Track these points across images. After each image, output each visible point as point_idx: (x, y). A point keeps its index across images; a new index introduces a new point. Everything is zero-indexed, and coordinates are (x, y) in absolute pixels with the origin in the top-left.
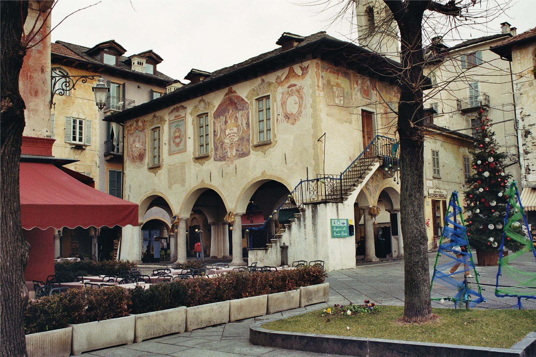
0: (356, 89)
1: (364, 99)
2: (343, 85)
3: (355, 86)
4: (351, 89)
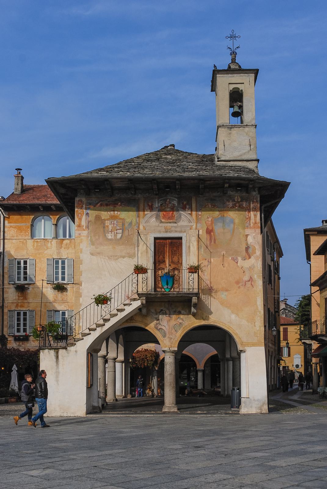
1: (161, 225)
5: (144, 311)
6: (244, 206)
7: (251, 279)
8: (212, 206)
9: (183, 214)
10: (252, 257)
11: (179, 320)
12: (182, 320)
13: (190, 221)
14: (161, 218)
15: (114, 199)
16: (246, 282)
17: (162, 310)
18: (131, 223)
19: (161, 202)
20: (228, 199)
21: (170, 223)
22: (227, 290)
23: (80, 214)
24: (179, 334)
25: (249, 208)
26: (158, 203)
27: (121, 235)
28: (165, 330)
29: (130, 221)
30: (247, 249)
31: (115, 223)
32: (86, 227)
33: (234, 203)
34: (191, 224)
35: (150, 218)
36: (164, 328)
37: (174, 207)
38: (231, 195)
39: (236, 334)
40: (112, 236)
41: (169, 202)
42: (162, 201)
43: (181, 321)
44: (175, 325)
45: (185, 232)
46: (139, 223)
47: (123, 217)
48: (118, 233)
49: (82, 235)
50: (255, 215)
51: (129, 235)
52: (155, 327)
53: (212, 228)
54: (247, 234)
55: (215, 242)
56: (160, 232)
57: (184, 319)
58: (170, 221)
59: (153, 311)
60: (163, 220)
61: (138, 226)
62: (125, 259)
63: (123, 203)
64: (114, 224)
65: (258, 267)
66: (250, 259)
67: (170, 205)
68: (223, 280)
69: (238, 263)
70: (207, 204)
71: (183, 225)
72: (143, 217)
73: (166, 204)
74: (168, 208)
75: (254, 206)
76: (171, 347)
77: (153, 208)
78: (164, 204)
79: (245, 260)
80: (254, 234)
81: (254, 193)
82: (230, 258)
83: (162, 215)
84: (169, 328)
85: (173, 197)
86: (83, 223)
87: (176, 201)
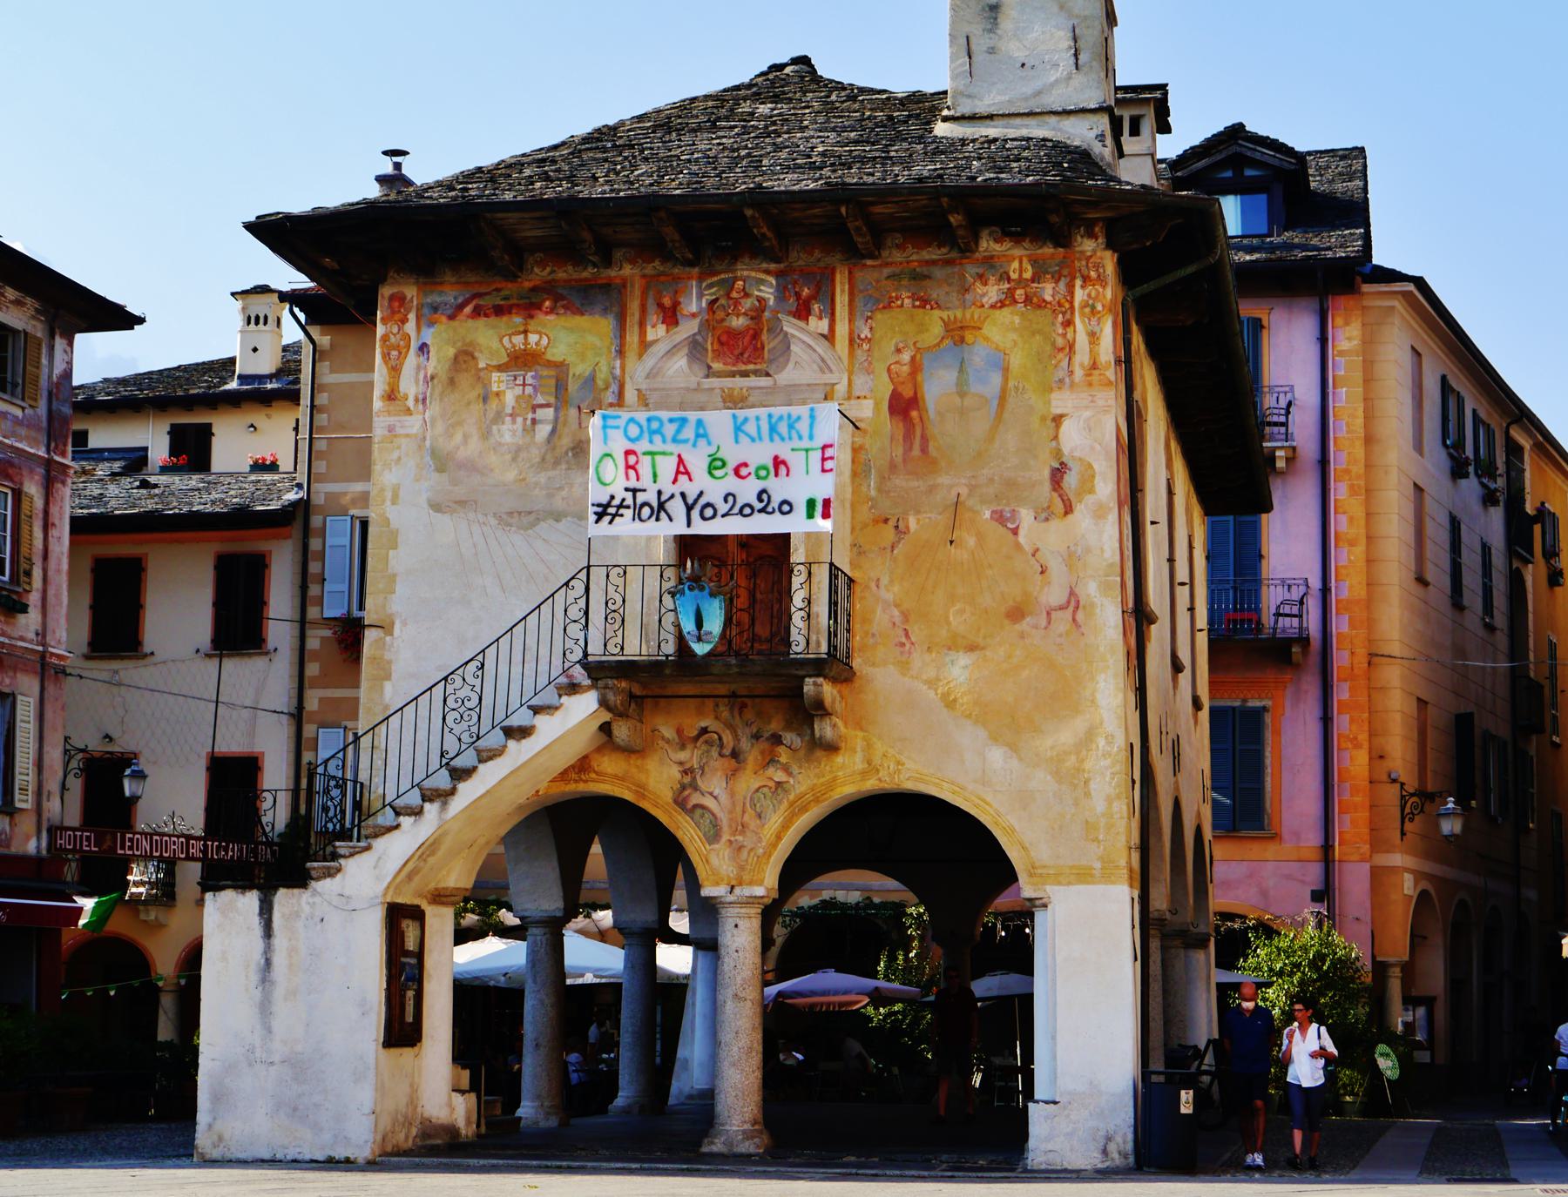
0: (659, 349)
2: (557, 353)
3: (657, 331)
4: (621, 353)
5: (622, 731)
6: (1048, 298)
7: (1073, 602)
10: (1079, 509)
11: (771, 771)
12: (786, 769)
13: (824, 367)
15: (527, 285)
16: (1054, 615)
17: (704, 731)
18: (591, 380)
20: (980, 271)
21: (745, 374)
22: (972, 648)
23: (397, 347)
24: (780, 832)
25: (1067, 305)
26: (700, 296)
27: (549, 428)
28: (719, 814)
30: (1058, 475)
31: (529, 380)
32: (417, 400)
34: (828, 378)
36: (708, 802)
38: (992, 257)
39: (1011, 831)
40: (514, 433)
43: (780, 776)
44: (757, 790)
47: (558, 358)
48: (541, 422)
49: (399, 431)
50: (1093, 337)
52: (676, 802)
54: (1059, 411)
55: (924, 450)
57: (795, 769)
58: (744, 367)
59: (668, 732)
62: (562, 525)
64: (524, 385)
65: (1102, 550)
66: (1070, 516)
67: (747, 304)
68: (958, 606)
69: (1022, 532)
72: (640, 356)
73: (729, 297)
74: (738, 316)
75: (1089, 295)
76: (740, 884)
78: (723, 301)
79: (1047, 519)
80: (1087, 414)
81: (1088, 245)
82: (987, 514)
84: (734, 804)
85: (759, 270)
86: (409, 386)
87: (771, 285)
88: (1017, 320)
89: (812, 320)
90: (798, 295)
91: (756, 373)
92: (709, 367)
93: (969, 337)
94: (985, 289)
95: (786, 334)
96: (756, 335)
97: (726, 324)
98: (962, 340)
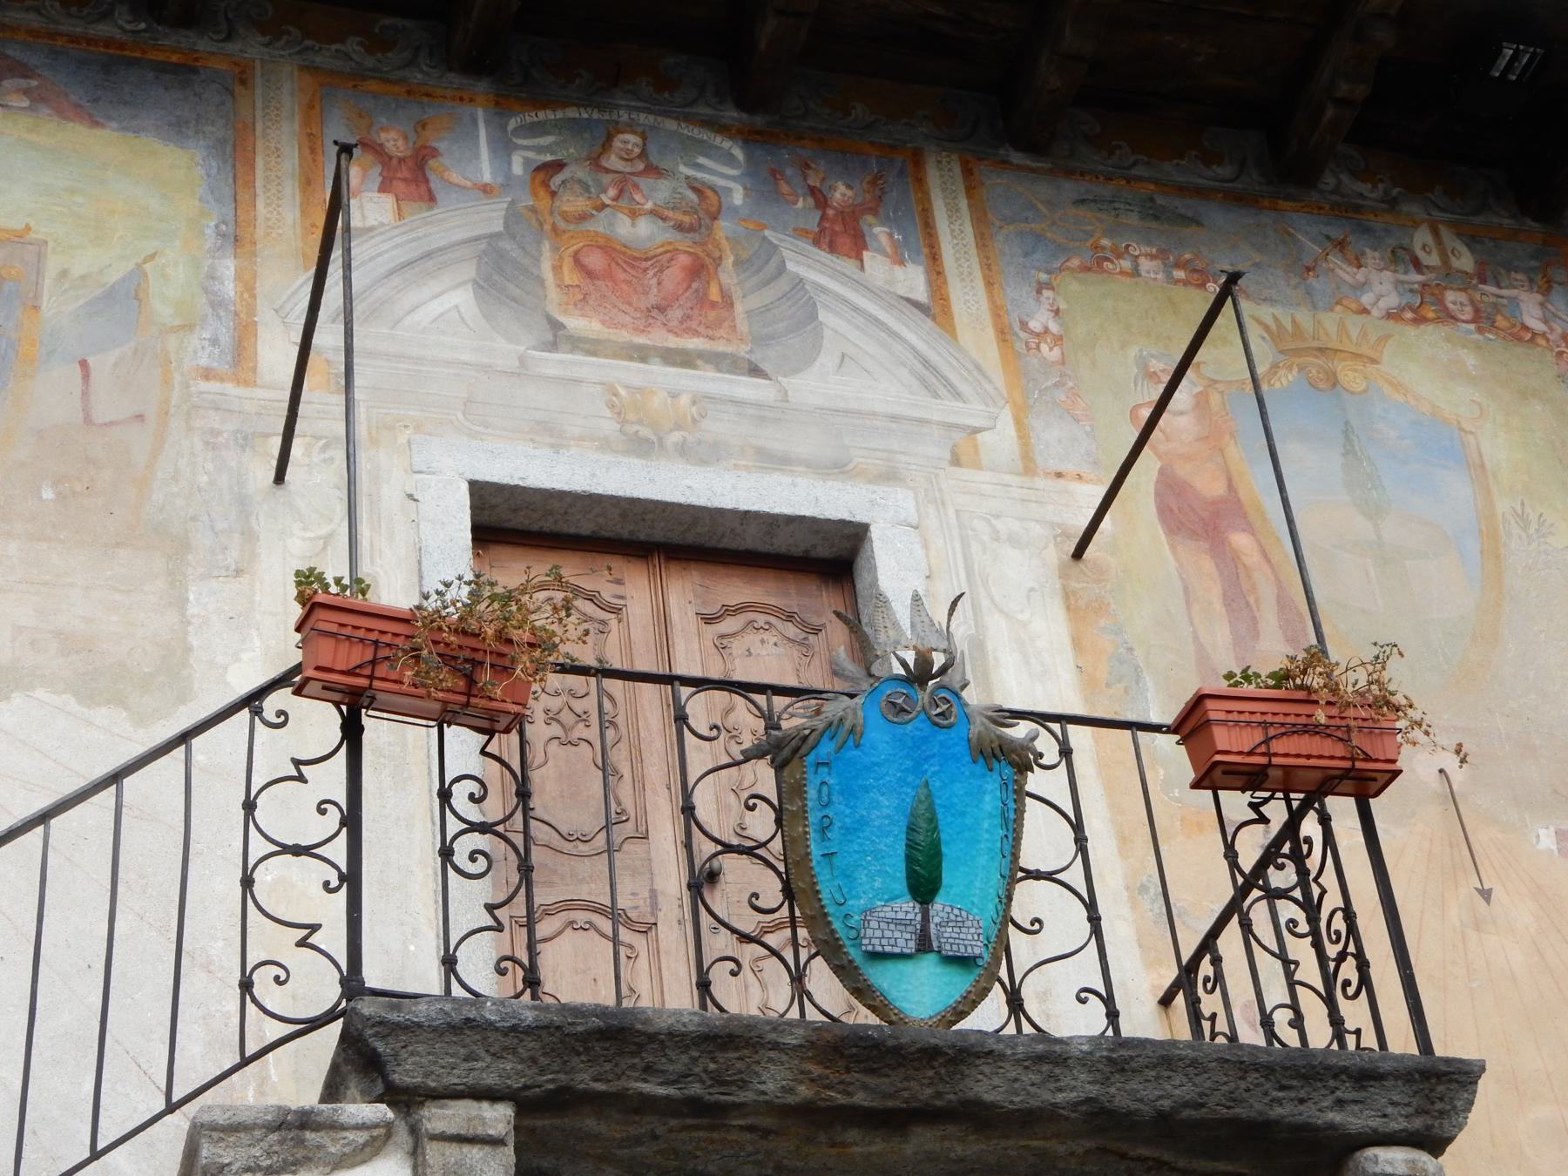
8: (1180, 274)
9: (845, 301)
13: (931, 379)
14: (553, 294)
18: (124, 298)
19: (540, 150)
21: (684, 359)
29: (114, 276)
33: (1419, 278)
35: (396, 280)
37: (715, 218)
41: (643, 155)
42: (549, 139)
45: (890, 476)
46: (252, 311)
51: (88, 420)
53: (1231, 486)
56: (550, 434)
58: (673, 342)
60: (576, 323)
61: (226, 338)
63: (23, 83)
70: (1105, 242)
71: (854, 405)
73: (595, 163)
74: (634, 214)
77: (435, 184)
82: (1547, 840)
83: (557, 269)
87: (730, 160)
88: (1470, 360)
89: (876, 265)
90: (820, 199)
91: (717, 361)
92: (556, 326)
93: (1350, 375)
94: (1361, 275)
95: (799, 282)
96: (699, 270)
97: (599, 225)
98: (1333, 381)
